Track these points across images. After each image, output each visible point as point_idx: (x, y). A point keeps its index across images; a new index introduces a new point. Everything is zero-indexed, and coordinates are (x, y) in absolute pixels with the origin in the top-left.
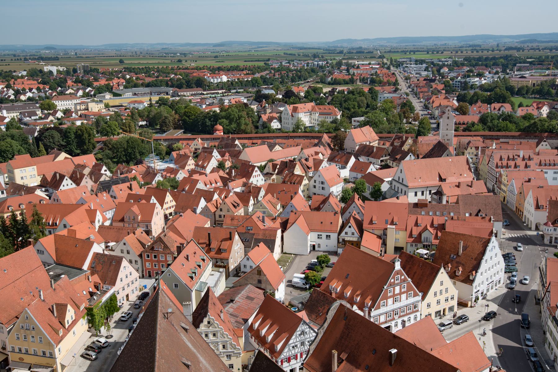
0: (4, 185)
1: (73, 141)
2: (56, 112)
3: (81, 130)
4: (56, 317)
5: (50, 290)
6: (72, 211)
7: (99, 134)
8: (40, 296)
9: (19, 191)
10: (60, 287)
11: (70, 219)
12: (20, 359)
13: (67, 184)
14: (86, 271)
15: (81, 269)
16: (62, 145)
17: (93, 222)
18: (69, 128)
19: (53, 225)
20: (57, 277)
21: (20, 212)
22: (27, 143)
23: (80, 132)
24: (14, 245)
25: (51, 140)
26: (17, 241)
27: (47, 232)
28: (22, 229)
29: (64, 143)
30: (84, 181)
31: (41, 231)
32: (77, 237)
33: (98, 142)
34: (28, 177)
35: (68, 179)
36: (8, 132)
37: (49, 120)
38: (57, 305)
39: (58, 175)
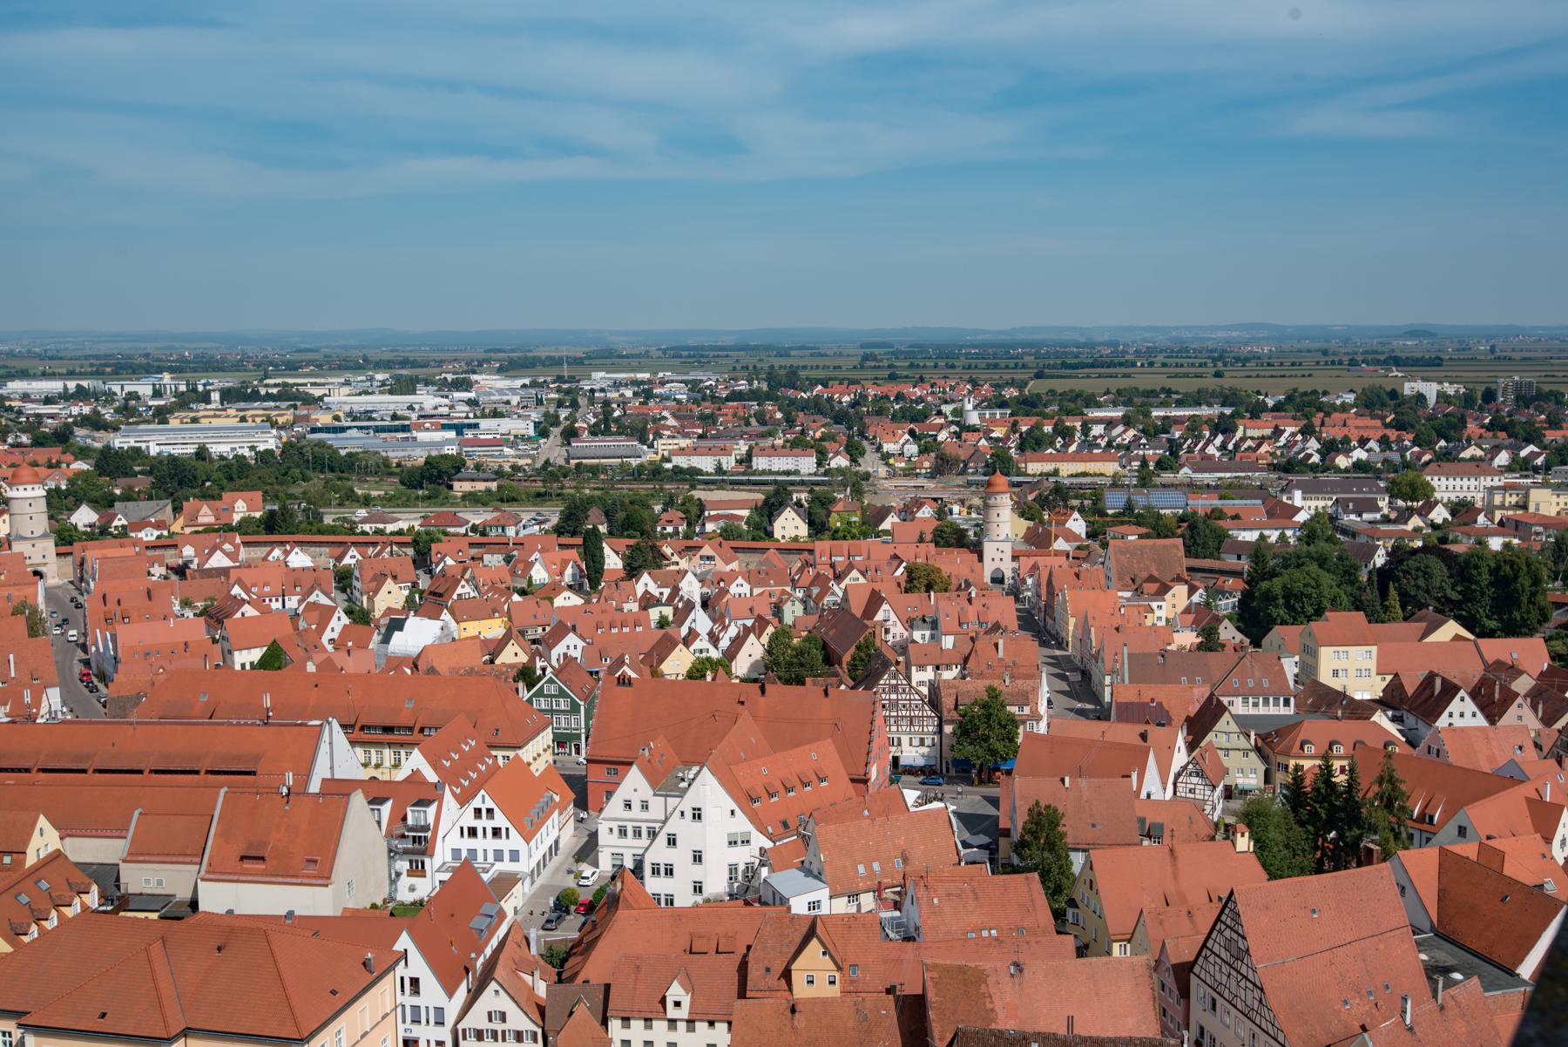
0: (1291, 683)
1: (1483, 594)
2: (1430, 506)
3: (1512, 563)
5: (1429, 1006)
6: (1497, 791)
7: (1558, 584)
8: (1404, 1012)
9: (1329, 705)
11: (1484, 815)
13: (1462, 713)
14: (1524, 983)
15: (1511, 972)
16: (1449, 600)
17: (1548, 840)
21: (1345, 763)
22: (1352, 583)
23: (1508, 568)
24: (1316, 848)
25: (1421, 582)
26: (1325, 840)
27: (1404, 835)
28: (1342, 809)
29: (1455, 596)
30: (1513, 711)
31: (1392, 830)
33: (1558, 605)
35: (1467, 699)
36: (1312, 548)
37: (1410, 527)
39: (1438, 682)
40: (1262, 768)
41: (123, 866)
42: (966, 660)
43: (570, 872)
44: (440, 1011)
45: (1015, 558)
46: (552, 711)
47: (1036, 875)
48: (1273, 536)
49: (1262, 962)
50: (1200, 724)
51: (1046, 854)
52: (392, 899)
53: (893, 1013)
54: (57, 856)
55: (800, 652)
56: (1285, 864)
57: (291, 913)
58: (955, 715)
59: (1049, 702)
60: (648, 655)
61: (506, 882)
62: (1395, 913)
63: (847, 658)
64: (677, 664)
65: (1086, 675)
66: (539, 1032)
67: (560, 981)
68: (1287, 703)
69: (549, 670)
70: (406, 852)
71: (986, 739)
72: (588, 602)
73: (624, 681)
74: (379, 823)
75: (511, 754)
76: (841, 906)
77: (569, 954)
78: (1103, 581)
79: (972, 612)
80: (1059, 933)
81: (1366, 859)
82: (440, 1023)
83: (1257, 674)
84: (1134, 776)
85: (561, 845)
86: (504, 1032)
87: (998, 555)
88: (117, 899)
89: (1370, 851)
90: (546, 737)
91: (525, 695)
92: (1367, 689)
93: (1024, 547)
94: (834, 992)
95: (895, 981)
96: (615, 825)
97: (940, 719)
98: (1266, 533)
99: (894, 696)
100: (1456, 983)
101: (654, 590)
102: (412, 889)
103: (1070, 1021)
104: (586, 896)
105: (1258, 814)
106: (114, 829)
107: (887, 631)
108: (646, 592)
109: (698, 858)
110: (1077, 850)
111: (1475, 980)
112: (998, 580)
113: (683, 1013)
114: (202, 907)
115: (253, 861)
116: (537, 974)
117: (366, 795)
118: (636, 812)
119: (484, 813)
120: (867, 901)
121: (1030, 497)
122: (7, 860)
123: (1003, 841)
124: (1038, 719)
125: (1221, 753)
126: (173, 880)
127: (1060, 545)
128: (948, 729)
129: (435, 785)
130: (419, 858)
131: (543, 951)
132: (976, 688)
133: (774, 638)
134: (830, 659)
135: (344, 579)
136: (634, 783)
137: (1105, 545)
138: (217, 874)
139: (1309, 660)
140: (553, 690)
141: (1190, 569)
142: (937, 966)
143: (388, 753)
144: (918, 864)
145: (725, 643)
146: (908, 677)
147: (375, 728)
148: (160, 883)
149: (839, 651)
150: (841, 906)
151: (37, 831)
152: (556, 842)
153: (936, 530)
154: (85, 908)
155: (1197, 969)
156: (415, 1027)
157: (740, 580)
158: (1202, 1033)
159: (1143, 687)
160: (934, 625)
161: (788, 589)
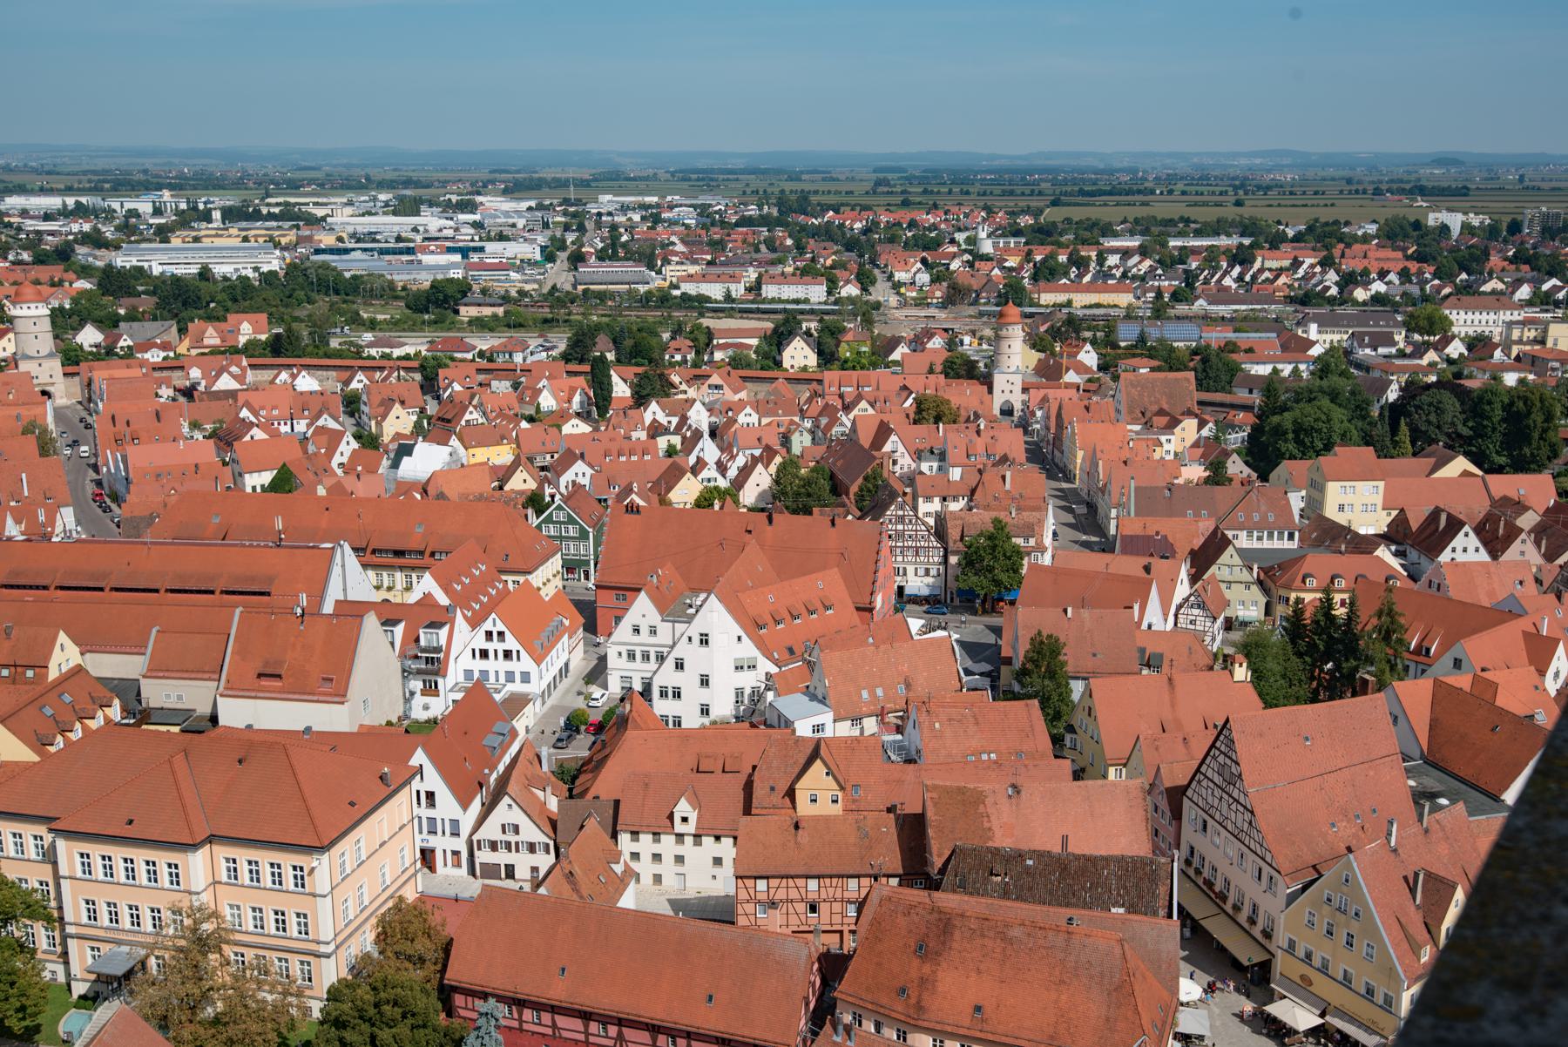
0: (1297, 518)
2: (1447, 340)
3: (1525, 400)
4: (1418, 907)
5: (1415, 829)
8: (1390, 834)
9: (1333, 540)
10: (1443, 829)
11: (1480, 649)
12: (1302, 977)
13: (1465, 548)
15: (1496, 798)
16: (1460, 436)
17: (1542, 673)
18: (1485, 390)
19: (1418, 651)
20: (1423, 797)
21: (1346, 596)
22: (1363, 418)
24: (1312, 678)
25: (1433, 418)
26: (1322, 670)
27: (1400, 666)
28: (1339, 641)
29: (1465, 432)
30: (1516, 546)
31: (1389, 661)
32: (1500, 702)
34: (1358, 508)
35: (1472, 534)
36: (1325, 383)
37: (1425, 361)
38: (1429, 875)
39: (1443, 517)
40: (1263, 600)
41: (143, 682)
42: (973, 492)
43: (579, 693)
44: (455, 823)
45: (1025, 390)
46: (561, 538)
47: (1036, 702)
48: (1286, 370)
49: (1253, 787)
50: (1204, 557)
51: (1047, 682)
52: (407, 717)
53: (893, 830)
54: (78, 670)
55: (808, 482)
56: (1281, 693)
57: (308, 729)
58: (960, 546)
59: (1055, 534)
60: (656, 483)
61: (517, 703)
62: (1386, 740)
63: (854, 489)
64: (685, 492)
65: (1092, 507)
66: (552, 843)
67: (571, 797)
68: (1291, 537)
69: (558, 497)
70: (419, 672)
71: (991, 569)
72: (596, 430)
73: (632, 509)
74: (392, 644)
75: (521, 579)
76: (845, 729)
77: (580, 771)
78: (1113, 414)
79: (980, 444)
80: (1056, 757)
81: (1360, 689)
82: (455, 834)
83: (1263, 508)
84: (1136, 607)
85: (571, 667)
86: (517, 844)
87: (1008, 387)
88: (140, 714)
89: (1365, 682)
90: (556, 563)
91: (534, 521)
92: (1371, 523)
93: (1034, 380)
94: (837, 809)
95: (896, 801)
96: (624, 649)
97: (946, 550)
98: (1280, 366)
99: (900, 527)
100: (1442, 807)
101: (662, 419)
102: (426, 708)
103: (1065, 839)
104: (595, 717)
105: (1257, 645)
107: (895, 462)
108: (655, 420)
109: (705, 681)
110: (1077, 678)
111: (1461, 806)
112: (1007, 412)
113: (691, 828)
115: (269, 679)
116: (549, 790)
117: (379, 616)
118: (644, 636)
119: (495, 635)
120: (871, 725)
121: (1043, 329)
122: (30, 673)
123: (1004, 670)
124: (1043, 550)
125: (1223, 586)
126: (194, 695)
127: (1071, 377)
128: (953, 560)
129: (447, 609)
130: (433, 678)
131: (554, 768)
132: (982, 519)
133: (782, 469)
134: (837, 489)
135: (352, 404)
136: (643, 609)
137: (1116, 378)
138: (235, 690)
139: (1315, 494)
140: (562, 516)
141: (1200, 403)
142: (935, 787)
143: (399, 575)
144: (921, 690)
145: (732, 472)
146: (915, 509)
147: (387, 551)
148: (180, 698)
149: (846, 481)
150: (845, 729)
152: (567, 665)
153: (946, 361)
154: (108, 721)
155: (1189, 793)
156: (431, 838)
157: (748, 410)
158: (1192, 853)
159: (1149, 520)
160: (942, 457)
161: (797, 419)
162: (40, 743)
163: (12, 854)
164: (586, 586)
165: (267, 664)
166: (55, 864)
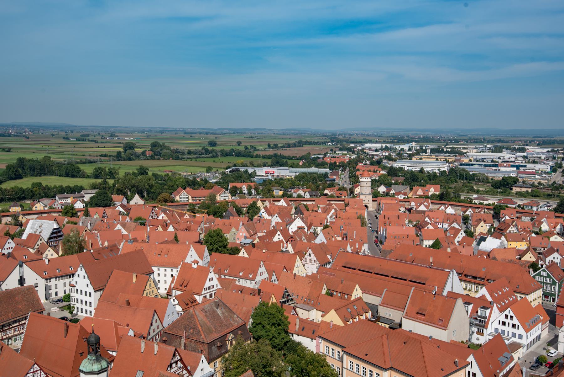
41: (380, 307)
43: (544, 349)
46: (543, 283)
52: (469, 341)
54: (360, 299)
57: (431, 337)
61: (516, 347)
69: (544, 266)
70: (476, 325)
74: (467, 312)
75: (524, 296)
85: (542, 337)
88: (377, 318)
90: (540, 292)
91: (532, 274)
102: (478, 339)
104: (551, 361)
106: (377, 293)
114: (403, 327)
115: (420, 315)
117: (463, 301)
122: (346, 296)
126: (395, 315)
130: (482, 328)
135: (465, 220)
138: (408, 316)
143: (473, 286)
147: (470, 276)
148: (390, 315)
151: (355, 290)
152: (540, 335)
154: (366, 317)
162: (345, 320)
163: (331, 355)
164: (552, 305)
165: (420, 309)
166: (343, 362)
